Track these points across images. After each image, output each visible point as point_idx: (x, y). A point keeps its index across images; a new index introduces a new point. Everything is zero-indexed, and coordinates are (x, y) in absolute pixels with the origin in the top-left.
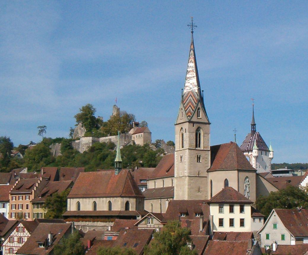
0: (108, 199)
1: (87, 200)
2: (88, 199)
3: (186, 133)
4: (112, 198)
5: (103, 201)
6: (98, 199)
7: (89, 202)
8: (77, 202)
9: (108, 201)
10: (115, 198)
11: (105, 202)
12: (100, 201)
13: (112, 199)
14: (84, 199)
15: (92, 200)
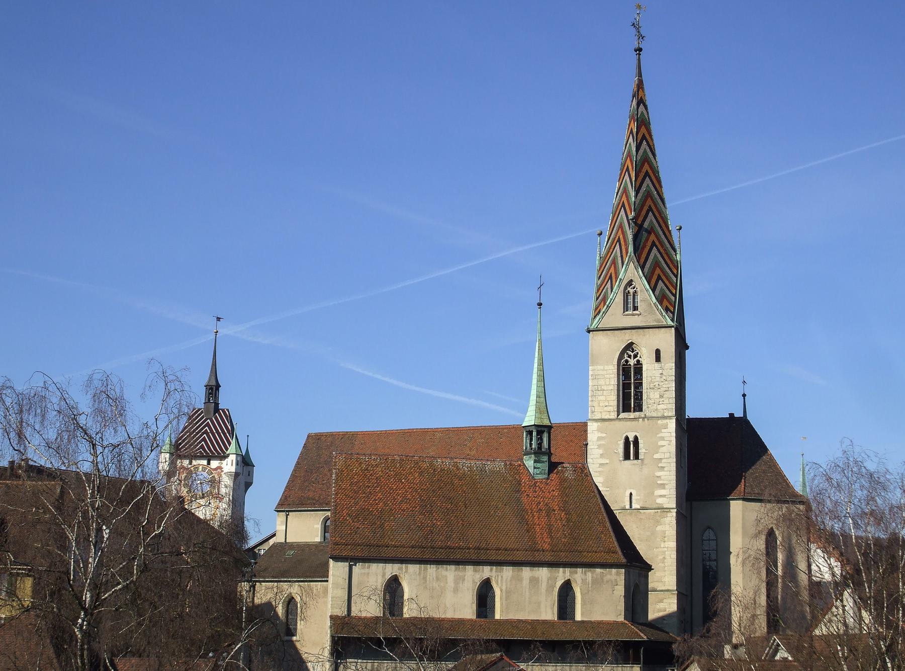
0: (562, 575)
1: (450, 572)
2: (453, 567)
3: (657, 365)
4: (579, 570)
5: (534, 581)
6: (508, 572)
7: (459, 580)
8: (388, 576)
9: (559, 583)
10: (598, 570)
11: (544, 585)
12: (520, 580)
13: (564, 572)
14: (432, 570)
15: (472, 576)
